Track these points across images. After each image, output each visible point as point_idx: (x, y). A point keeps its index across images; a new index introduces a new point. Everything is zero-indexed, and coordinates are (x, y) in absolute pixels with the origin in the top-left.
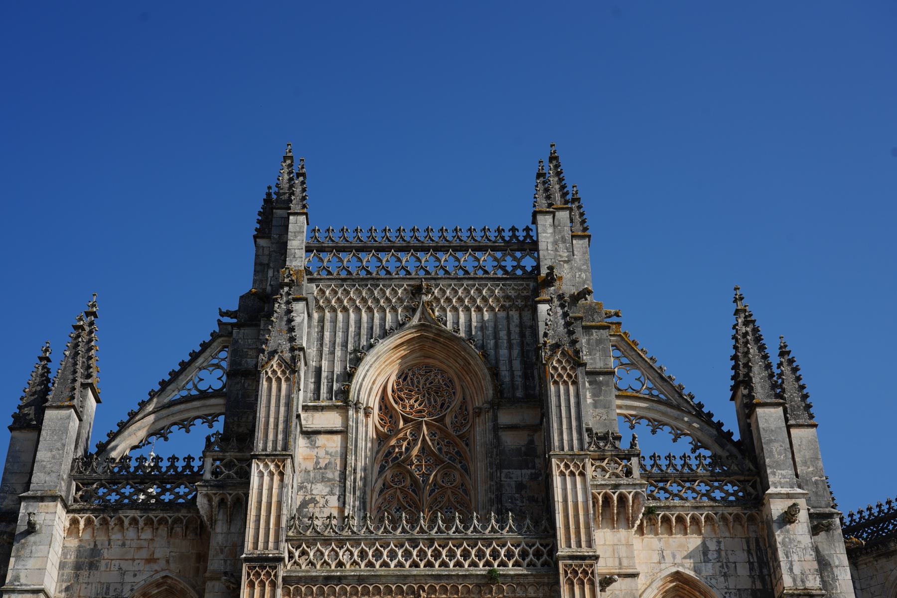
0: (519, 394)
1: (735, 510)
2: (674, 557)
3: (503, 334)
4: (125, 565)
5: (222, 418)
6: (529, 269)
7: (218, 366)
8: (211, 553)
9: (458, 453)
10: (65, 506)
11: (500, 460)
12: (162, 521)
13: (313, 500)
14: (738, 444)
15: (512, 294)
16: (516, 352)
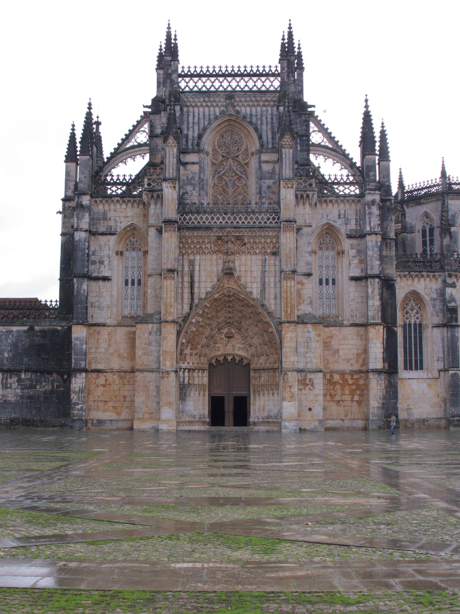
0: (270, 146)
1: (352, 198)
3: (264, 118)
4: (117, 219)
5: (148, 155)
6: (276, 87)
7: (144, 131)
8: (150, 217)
9: (244, 171)
10: (92, 196)
11: (261, 177)
12: (129, 201)
13: (186, 193)
14: (358, 168)
15: (269, 99)
16: (269, 127)
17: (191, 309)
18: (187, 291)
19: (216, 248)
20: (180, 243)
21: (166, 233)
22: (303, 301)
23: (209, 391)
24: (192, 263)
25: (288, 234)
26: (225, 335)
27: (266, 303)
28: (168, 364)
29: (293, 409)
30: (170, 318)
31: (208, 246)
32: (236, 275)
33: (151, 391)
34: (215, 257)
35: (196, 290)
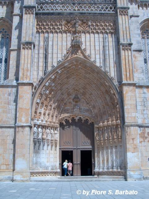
2: (147, 15)
17: (45, 74)
18: (42, 60)
19: (66, 29)
20: (37, 25)
21: (26, 15)
22: (137, 70)
23: (60, 146)
24: (46, 40)
25: (123, 17)
26: (73, 100)
27: (107, 69)
28: (23, 119)
29: (136, 160)
30: (25, 81)
31: (60, 27)
32: (83, 47)
33: (8, 145)
34: (64, 35)
35: (50, 60)
